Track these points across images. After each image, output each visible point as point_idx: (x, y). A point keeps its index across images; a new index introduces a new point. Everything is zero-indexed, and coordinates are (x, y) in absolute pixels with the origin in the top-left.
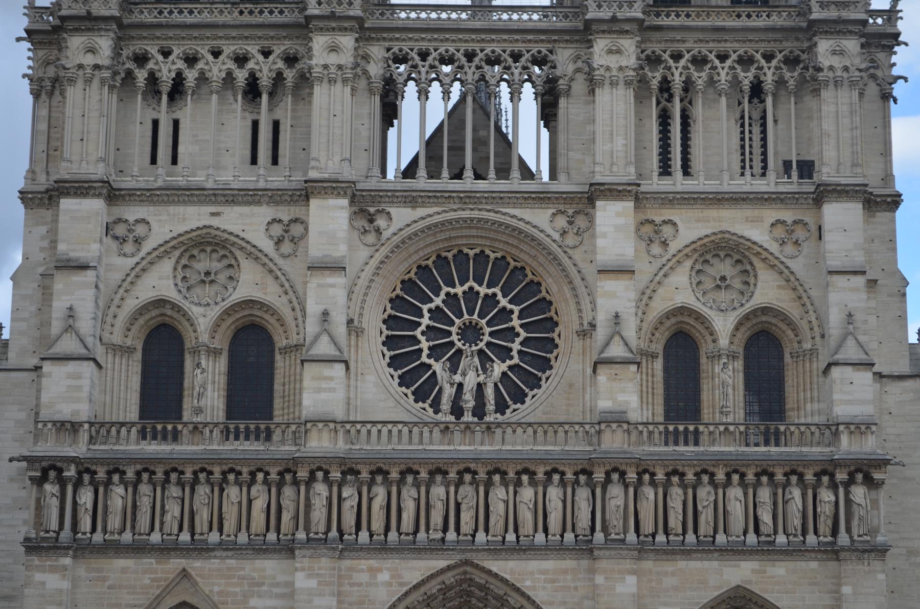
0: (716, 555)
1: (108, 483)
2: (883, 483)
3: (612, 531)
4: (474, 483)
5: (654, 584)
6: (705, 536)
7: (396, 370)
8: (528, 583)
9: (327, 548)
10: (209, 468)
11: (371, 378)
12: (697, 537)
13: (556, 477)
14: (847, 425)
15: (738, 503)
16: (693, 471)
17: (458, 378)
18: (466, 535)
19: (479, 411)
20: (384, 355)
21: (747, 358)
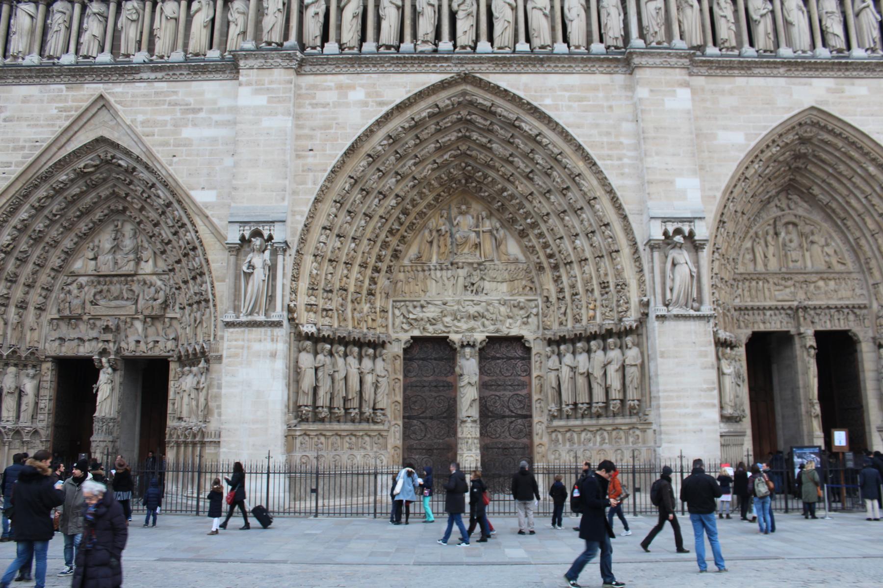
0: (782, 70)
8: (548, 101)
12: (757, 51)
15: (800, 13)
18: (464, 47)
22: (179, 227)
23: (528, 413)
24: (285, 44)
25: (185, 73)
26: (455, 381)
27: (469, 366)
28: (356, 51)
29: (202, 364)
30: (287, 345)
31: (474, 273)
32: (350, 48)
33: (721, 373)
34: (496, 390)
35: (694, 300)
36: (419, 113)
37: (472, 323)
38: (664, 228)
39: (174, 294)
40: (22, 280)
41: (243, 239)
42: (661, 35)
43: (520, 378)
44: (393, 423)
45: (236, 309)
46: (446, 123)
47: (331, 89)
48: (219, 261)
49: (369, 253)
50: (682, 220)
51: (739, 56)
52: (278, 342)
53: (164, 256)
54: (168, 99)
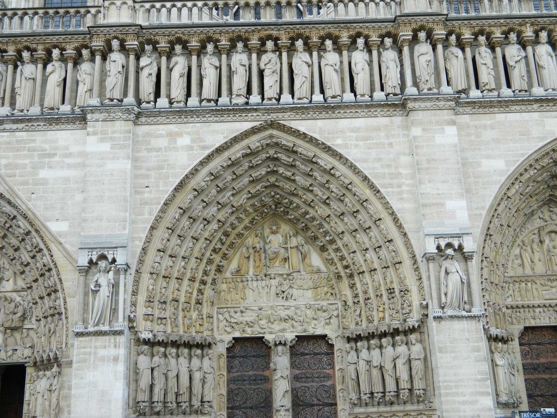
0: (536, 106)
3: (424, 86)
4: (278, 49)
8: (339, 141)
12: (514, 92)
13: (361, 41)
16: (499, 31)
18: (270, 99)
22: (37, 252)
23: (333, 402)
24: (125, 100)
25: (42, 124)
26: (271, 375)
27: (281, 362)
28: (182, 104)
29: (55, 369)
30: (128, 350)
31: (284, 282)
32: (178, 102)
33: (494, 364)
34: (305, 382)
35: (465, 303)
36: (234, 154)
37: (284, 325)
38: (437, 243)
39: (31, 308)
41: (91, 262)
42: (432, 83)
43: (325, 371)
44: (219, 413)
45: (85, 321)
46: (257, 161)
47: (163, 137)
48: (70, 280)
49: (196, 269)
50: (453, 236)
51: (499, 96)
53: (23, 276)
54: (27, 146)
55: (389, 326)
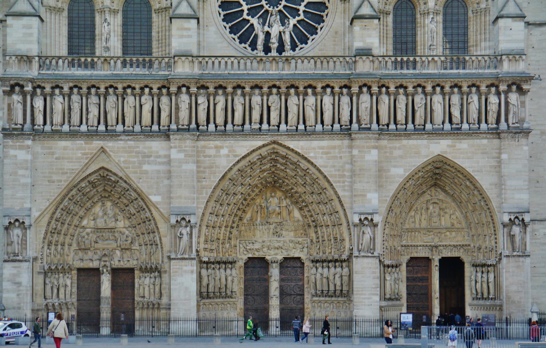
0: (426, 136)
1: (52, 95)
2: (529, 91)
4: (279, 93)
5: (388, 154)
6: (419, 125)
7: (227, 23)
8: (312, 155)
9: (190, 135)
10: (115, 85)
11: (213, 29)
12: (414, 126)
13: (329, 90)
14: (508, 55)
15: (439, 105)
16: (412, 86)
17: (266, 28)
18: (274, 126)
19: (281, 49)
20: (220, 14)
21: (445, 15)
25: (143, 137)
29: (156, 274)
40: (63, 232)
47: (212, 148)
48: (163, 227)
52: (193, 266)
55: (333, 257)
